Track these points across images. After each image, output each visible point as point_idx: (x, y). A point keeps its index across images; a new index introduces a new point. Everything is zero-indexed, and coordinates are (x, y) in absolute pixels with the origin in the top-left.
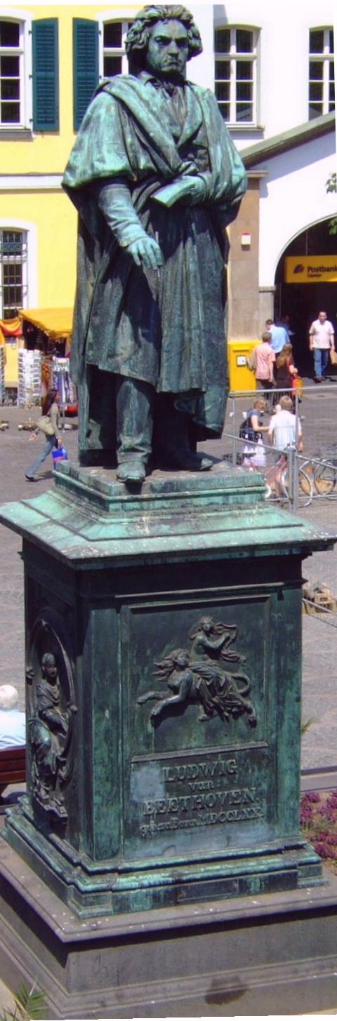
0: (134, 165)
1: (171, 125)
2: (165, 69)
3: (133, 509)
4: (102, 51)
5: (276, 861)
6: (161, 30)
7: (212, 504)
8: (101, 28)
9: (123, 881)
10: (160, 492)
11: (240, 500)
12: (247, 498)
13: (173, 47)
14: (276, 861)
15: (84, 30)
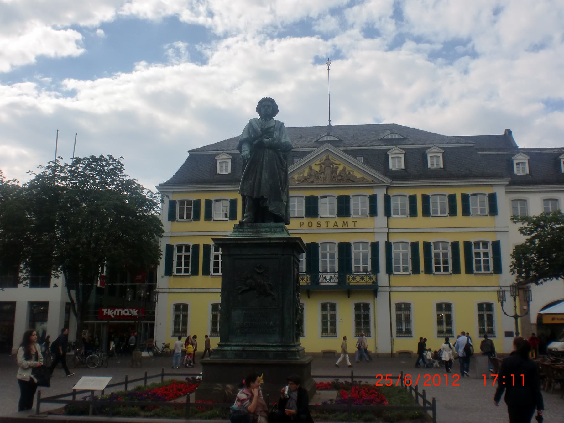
0: (250, 136)
1: (262, 126)
2: (264, 114)
3: (241, 231)
4: (474, 251)
5: (280, 349)
6: (263, 104)
7: (266, 231)
8: (473, 243)
9: (226, 348)
10: (250, 226)
11: (275, 230)
12: (278, 230)
13: (266, 107)
14: (280, 349)
15: (467, 245)
